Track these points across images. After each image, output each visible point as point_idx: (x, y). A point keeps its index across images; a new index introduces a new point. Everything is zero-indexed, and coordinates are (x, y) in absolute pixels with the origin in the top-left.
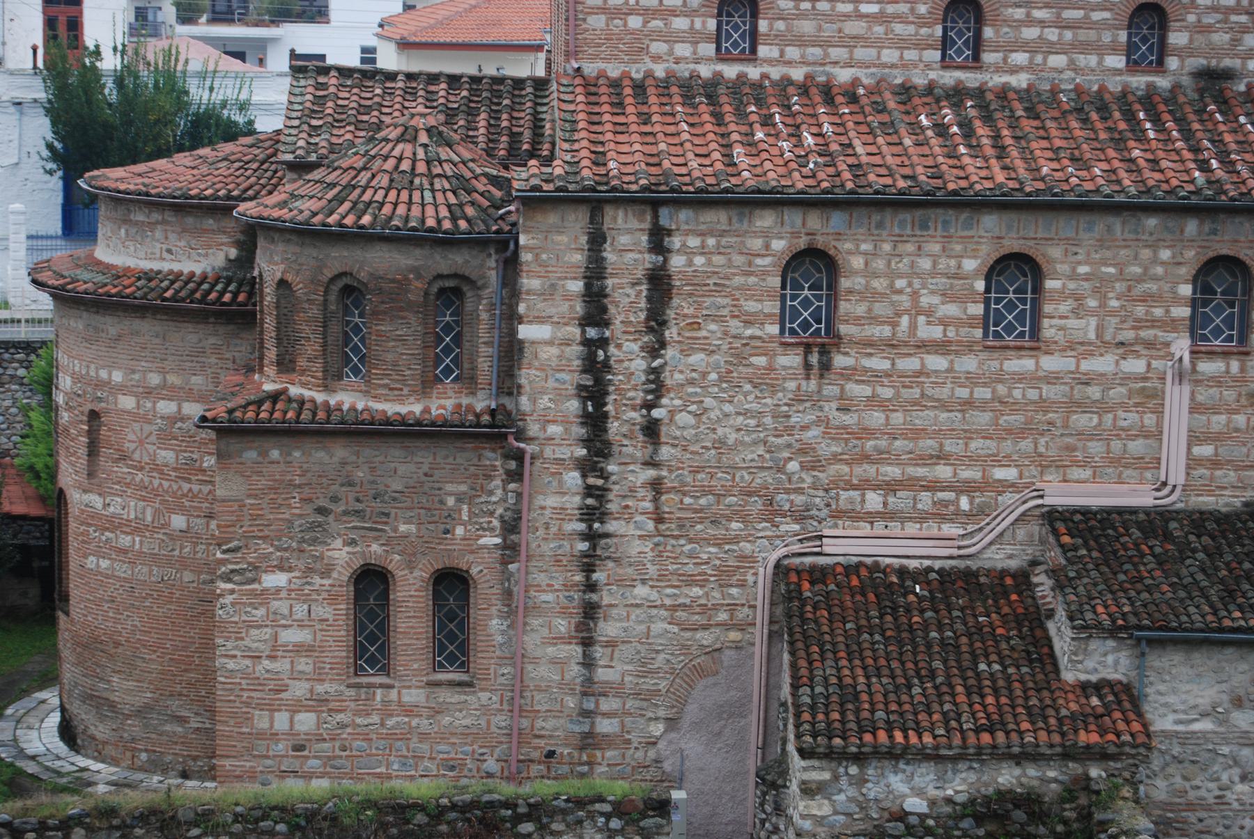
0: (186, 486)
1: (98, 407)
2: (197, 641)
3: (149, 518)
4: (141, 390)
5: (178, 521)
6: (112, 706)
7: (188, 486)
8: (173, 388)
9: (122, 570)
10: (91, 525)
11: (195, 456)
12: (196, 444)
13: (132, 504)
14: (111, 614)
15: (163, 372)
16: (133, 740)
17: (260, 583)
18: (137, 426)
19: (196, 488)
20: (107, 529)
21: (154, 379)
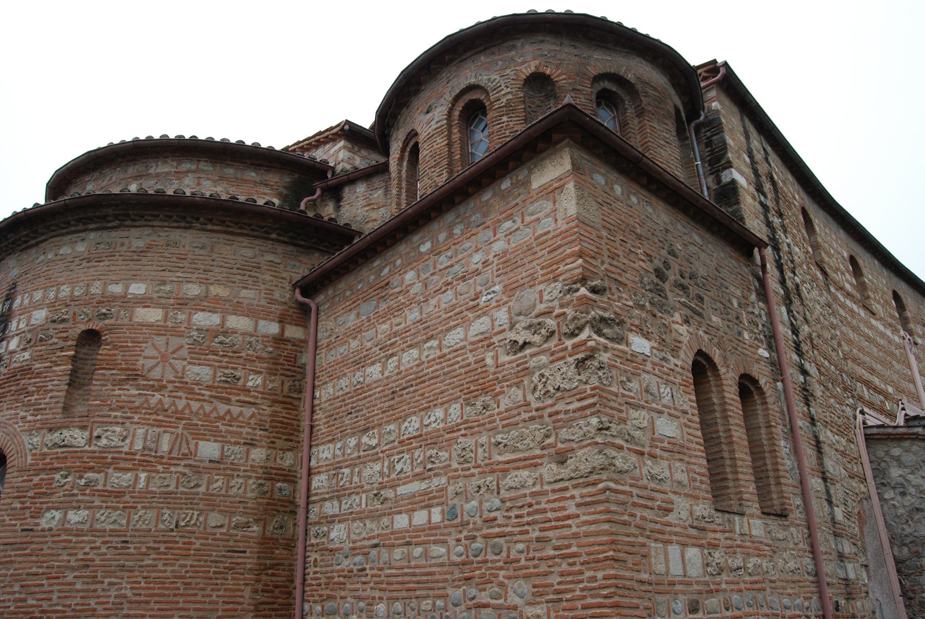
0: (222, 408)
1: (96, 325)
2: (220, 606)
3: (165, 447)
4: (172, 301)
5: (209, 449)
7: (227, 407)
8: (217, 299)
9: (108, 519)
10: (58, 469)
11: (238, 374)
12: (241, 361)
13: (141, 432)
14: (78, 586)
15: (205, 282)
17: (628, 344)
18: (160, 341)
19: (235, 410)
20: (91, 469)
21: (194, 290)
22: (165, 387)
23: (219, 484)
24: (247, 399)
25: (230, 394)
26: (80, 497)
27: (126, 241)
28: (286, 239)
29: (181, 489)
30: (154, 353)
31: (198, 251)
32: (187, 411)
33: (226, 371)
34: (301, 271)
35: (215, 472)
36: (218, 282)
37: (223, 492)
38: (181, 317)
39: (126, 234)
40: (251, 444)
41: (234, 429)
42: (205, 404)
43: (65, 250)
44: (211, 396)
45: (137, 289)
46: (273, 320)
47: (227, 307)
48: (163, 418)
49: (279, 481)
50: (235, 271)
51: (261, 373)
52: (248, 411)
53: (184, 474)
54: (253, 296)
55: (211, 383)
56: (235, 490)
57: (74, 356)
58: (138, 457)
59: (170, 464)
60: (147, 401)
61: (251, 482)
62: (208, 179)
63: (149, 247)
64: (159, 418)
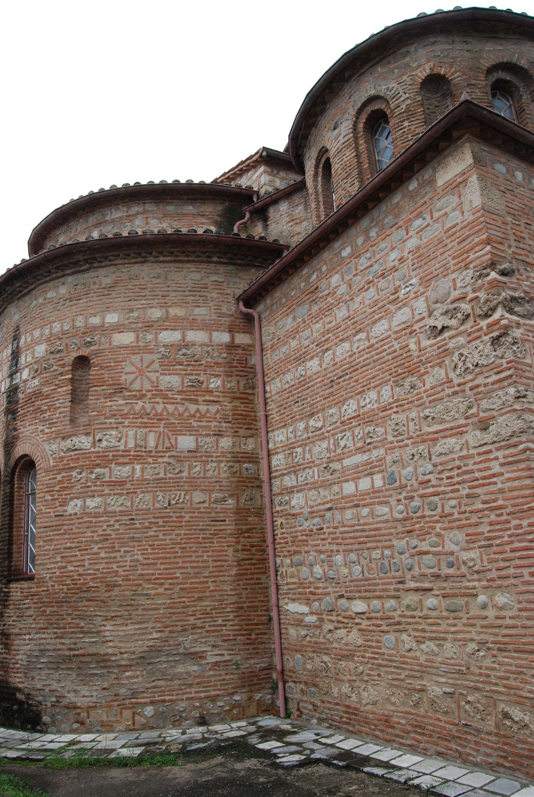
0: (193, 408)
1: (84, 352)
2: (211, 564)
3: (152, 443)
4: (140, 325)
5: (186, 442)
6: (103, 661)
7: (196, 407)
8: (176, 318)
9: (117, 503)
10: (74, 468)
11: (201, 379)
12: (202, 368)
13: (131, 433)
14: (103, 555)
15: (164, 306)
16: (134, 694)
18: (136, 359)
19: (203, 408)
20: (98, 465)
21: (156, 313)
22: (144, 395)
23: (198, 468)
24: (211, 398)
25: (197, 396)
26: (94, 488)
27: (97, 280)
28: (225, 261)
29: (169, 475)
30: (133, 369)
31: (155, 281)
32: (165, 413)
33: (191, 378)
34: (242, 286)
35: (193, 459)
36: (175, 305)
37: (202, 475)
38: (150, 337)
39: (95, 274)
40: (219, 435)
41: (204, 424)
42: (178, 406)
43: (51, 294)
44: (182, 399)
45: (112, 318)
46: (224, 331)
47: (185, 324)
48: (147, 421)
49: (245, 462)
50: (187, 293)
51: (219, 376)
52: (213, 409)
53: (170, 463)
54: (204, 313)
55: (180, 389)
56: (211, 473)
57: (72, 379)
58: (132, 453)
59: (158, 457)
60: (132, 408)
61: (223, 465)
62: (154, 218)
63: (116, 283)
64: (144, 420)
